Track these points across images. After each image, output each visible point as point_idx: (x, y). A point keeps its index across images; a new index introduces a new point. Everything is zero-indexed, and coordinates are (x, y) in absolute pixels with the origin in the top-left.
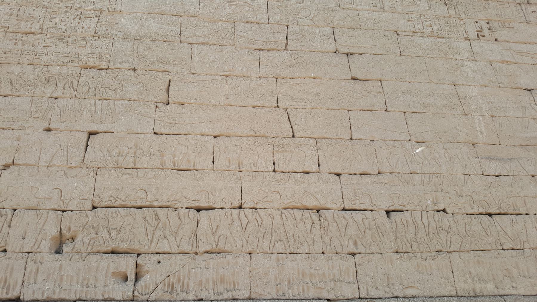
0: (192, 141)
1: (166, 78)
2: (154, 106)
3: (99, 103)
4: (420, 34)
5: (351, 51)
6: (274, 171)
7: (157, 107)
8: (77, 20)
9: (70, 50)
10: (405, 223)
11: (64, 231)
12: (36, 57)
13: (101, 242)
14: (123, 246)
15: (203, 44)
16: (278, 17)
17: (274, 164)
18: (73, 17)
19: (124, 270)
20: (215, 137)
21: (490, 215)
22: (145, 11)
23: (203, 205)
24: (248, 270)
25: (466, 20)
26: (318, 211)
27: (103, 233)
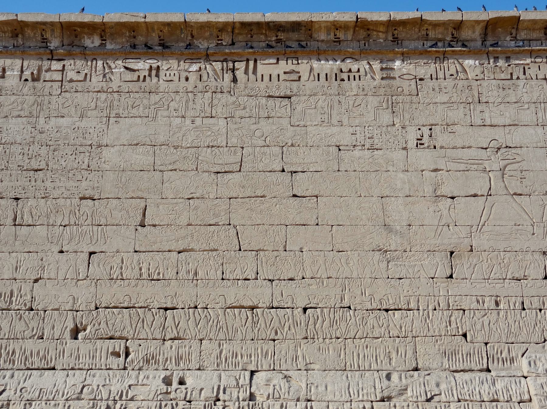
0: (162, 257)
1: (143, 205)
2: (134, 230)
3: (95, 228)
4: (360, 148)
5: (294, 170)
6: (223, 279)
7: (136, 230)
8: (74, 156)
9: (72, 183)
10: (316, 318)
11: (79, 326)
12: (47, 192)
13: (103, 332)
14: (117, 334)
15: (171, 170)
16: (233, 141)
17: (223, 273)
18: (70, 154)
19: (118, 350)
20: (179, 252)
21: (387, 310)
22: (126, 143)
23: (169, 305)
24: (199, 352)
25: (408, 129)
26: (253, 309)
27: (103, 325)
